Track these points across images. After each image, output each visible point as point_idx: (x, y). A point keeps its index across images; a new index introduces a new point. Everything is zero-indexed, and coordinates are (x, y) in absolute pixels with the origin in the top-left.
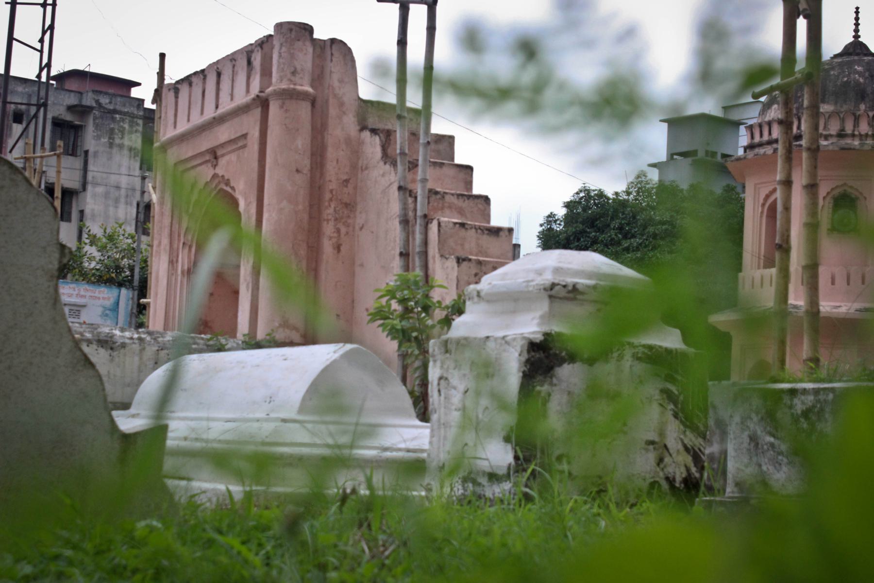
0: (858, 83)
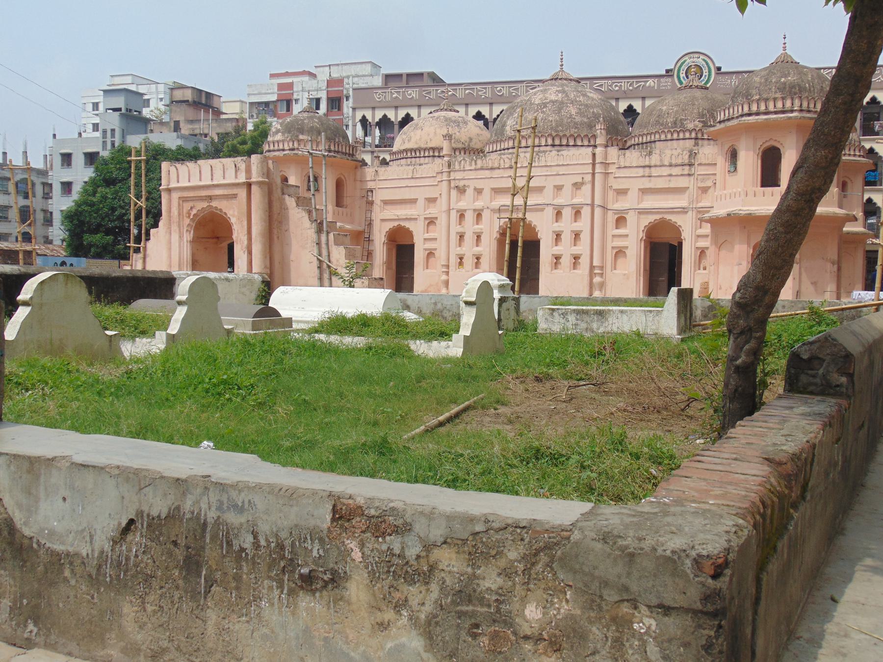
0: (317, 127)
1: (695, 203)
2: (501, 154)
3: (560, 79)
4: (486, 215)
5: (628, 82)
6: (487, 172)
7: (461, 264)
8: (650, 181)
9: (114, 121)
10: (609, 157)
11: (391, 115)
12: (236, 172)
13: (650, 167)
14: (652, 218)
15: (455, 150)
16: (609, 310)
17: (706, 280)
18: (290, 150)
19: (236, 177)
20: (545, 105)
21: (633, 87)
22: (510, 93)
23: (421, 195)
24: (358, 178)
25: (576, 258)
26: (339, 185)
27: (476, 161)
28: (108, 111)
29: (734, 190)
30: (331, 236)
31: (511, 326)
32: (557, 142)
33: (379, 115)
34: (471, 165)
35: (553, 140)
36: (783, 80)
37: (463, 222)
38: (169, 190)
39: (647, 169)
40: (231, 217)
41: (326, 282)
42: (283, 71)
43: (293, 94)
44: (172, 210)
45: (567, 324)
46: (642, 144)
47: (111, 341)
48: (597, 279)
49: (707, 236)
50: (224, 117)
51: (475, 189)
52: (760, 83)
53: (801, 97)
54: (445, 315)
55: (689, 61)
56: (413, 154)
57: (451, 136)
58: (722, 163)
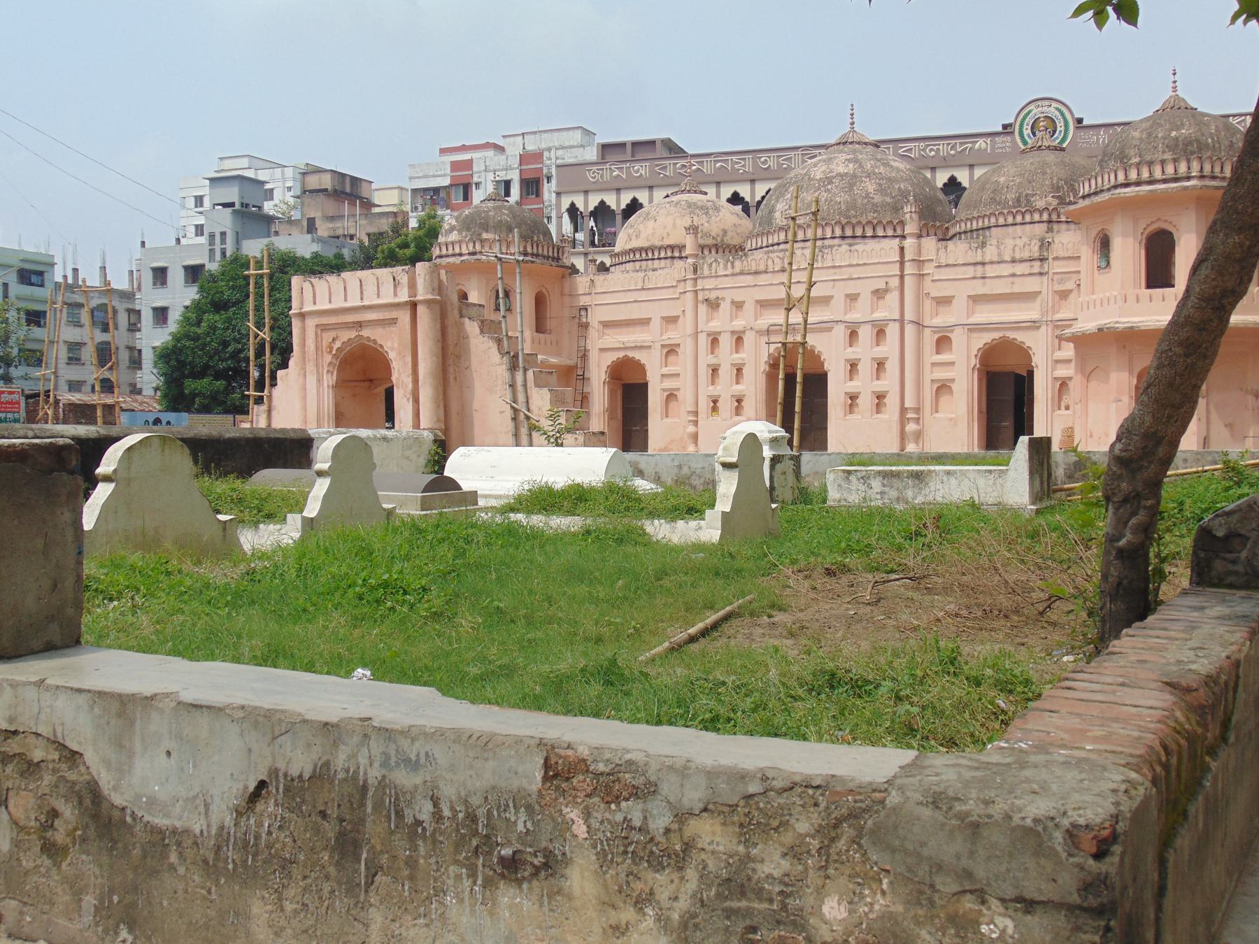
0: (507, 221)
1: (1050, 313)
2: (768, 252)
3: (851, 143)
4: (749, 338)
5: (948, 144)
6: (749, 277)
7: (715, 409)
9: (224, 221)
10: (924, 251)
11: (611, 200)
12: (395, 287)
13: (983, 264)
14: (988, 338)
15: (702, 247)
16: (930, 471)
17: (1070, 425)
18: (470, 254)
19: (395, 295)
20: (830, 181)
21: (956, 150)
22: (780, 165)
23: (655, 313)
24: (566, 291)
25: (880, 397)
26: (540, 302)
27: (732, 263)
28: (217, 207)
29: (1107, 294)
30: (530, 374)
31: (788, 496)
32: (849, 232)
33: (594, 201)
34: (726, 268)
35: (843, 229)
36: (1174, 134)
37: (716, 351)
38: (302, 316)
39: (979, 268)
40: (389, 351)
41: (524, 438)
42: (458, 144)
43: (472, 175)
45: (870, 492)
46: (972, 231)
47: (224, 529)
48: (911, 427)
49: (1069, 361)
50: (376, 210)
51: (733, 302)
52: (1141, 139)
53: (1200, 158)
54: (694, 483)
55: (1036, 111)
56: (644, 255)
57: (697, 228)
58: (1088, 255)
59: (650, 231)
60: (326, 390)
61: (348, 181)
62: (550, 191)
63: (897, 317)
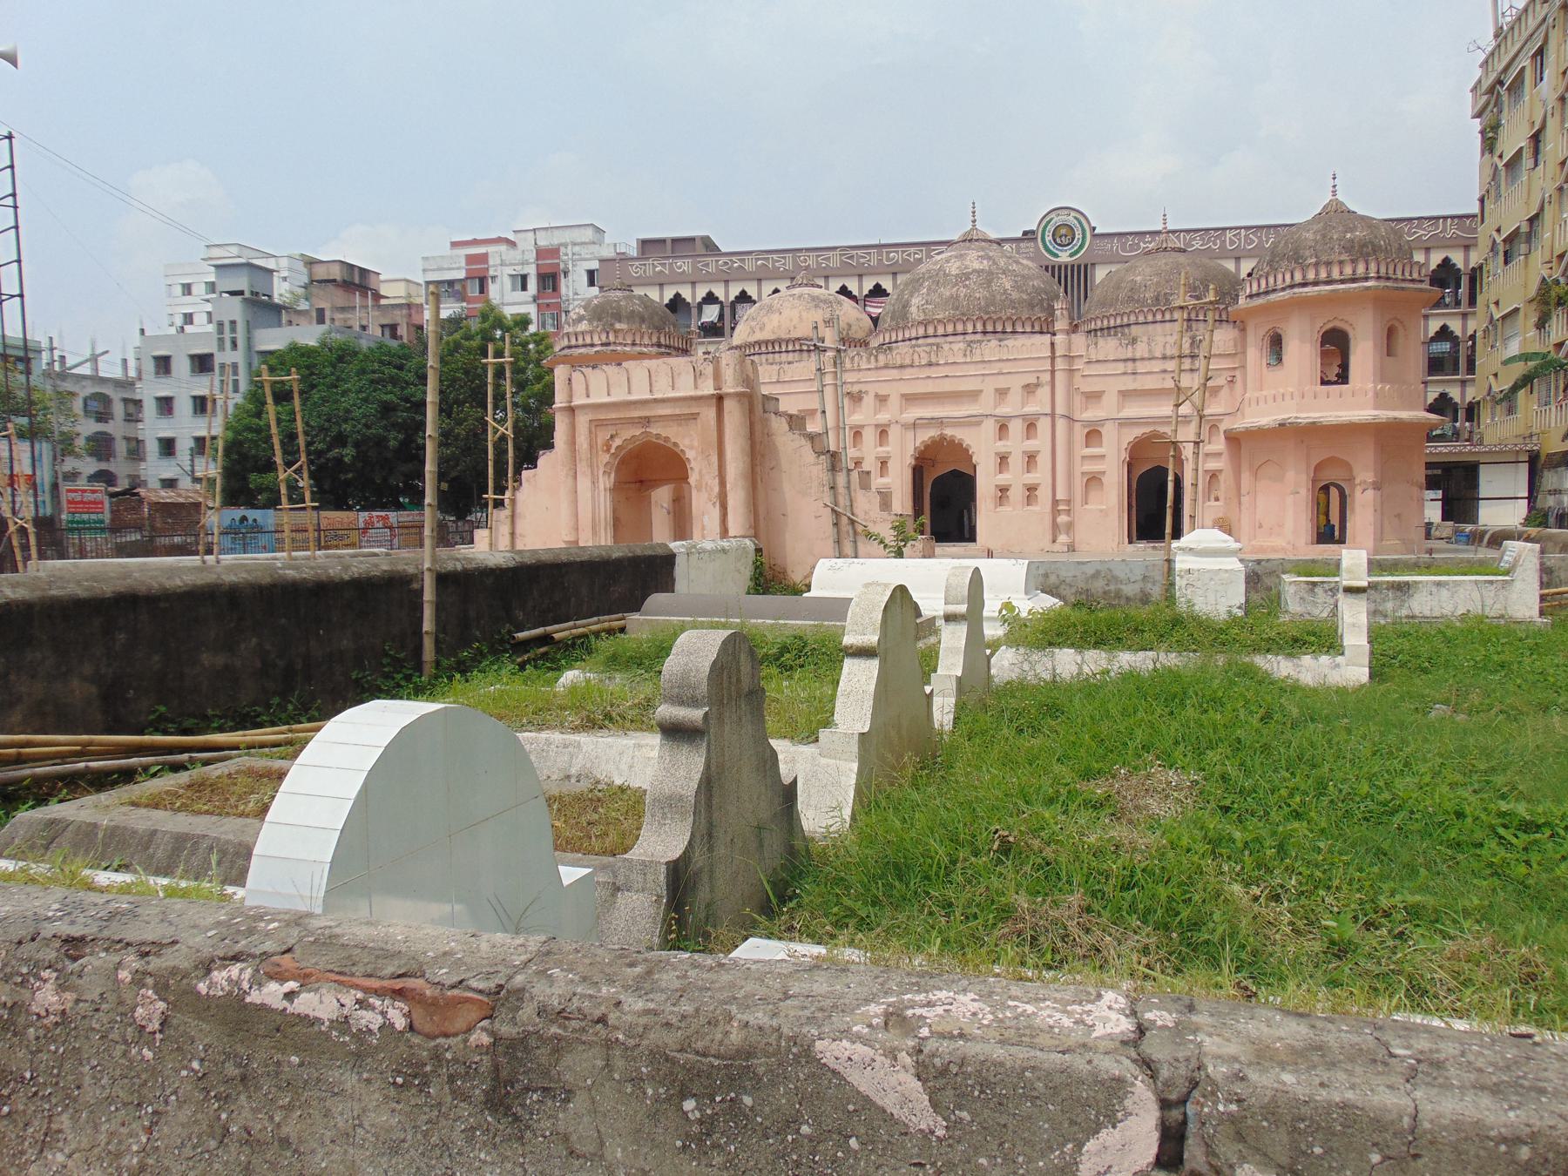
2: (914, 346)
4: (894, 433)
8: (1135, 380)
9: (234, 310)
11: (686, 294)
13: (1134, 360)
16: (1415, 582)
18: (602, 345)
25: (1031, 489)
27: (876, 357)
28: (225, 295)
29: (1282, 391)
32: (989, 328)
33: (669, 294)
34: (869, 361)
36: (1348, 235)
39: (1130, 364)
40: (687, 451)
41: (848, 547)
42: (469, 238)
44: (578, 440)
46: (1109, 328)
49: (1220, 454)
50: (383, 302)
51: (877, 396)
54: (1064, 593)
55: (1057, 220)
56: (770, 349)
58: (1255, 355)
59: (775, 323)
60: (602, 493)
61: (356, 271)
62: (567, 287)
63: (1048, 411)
